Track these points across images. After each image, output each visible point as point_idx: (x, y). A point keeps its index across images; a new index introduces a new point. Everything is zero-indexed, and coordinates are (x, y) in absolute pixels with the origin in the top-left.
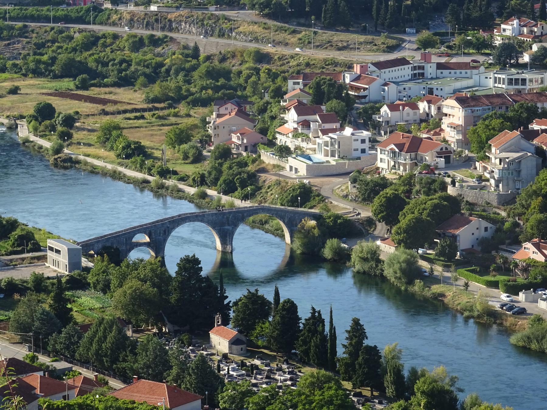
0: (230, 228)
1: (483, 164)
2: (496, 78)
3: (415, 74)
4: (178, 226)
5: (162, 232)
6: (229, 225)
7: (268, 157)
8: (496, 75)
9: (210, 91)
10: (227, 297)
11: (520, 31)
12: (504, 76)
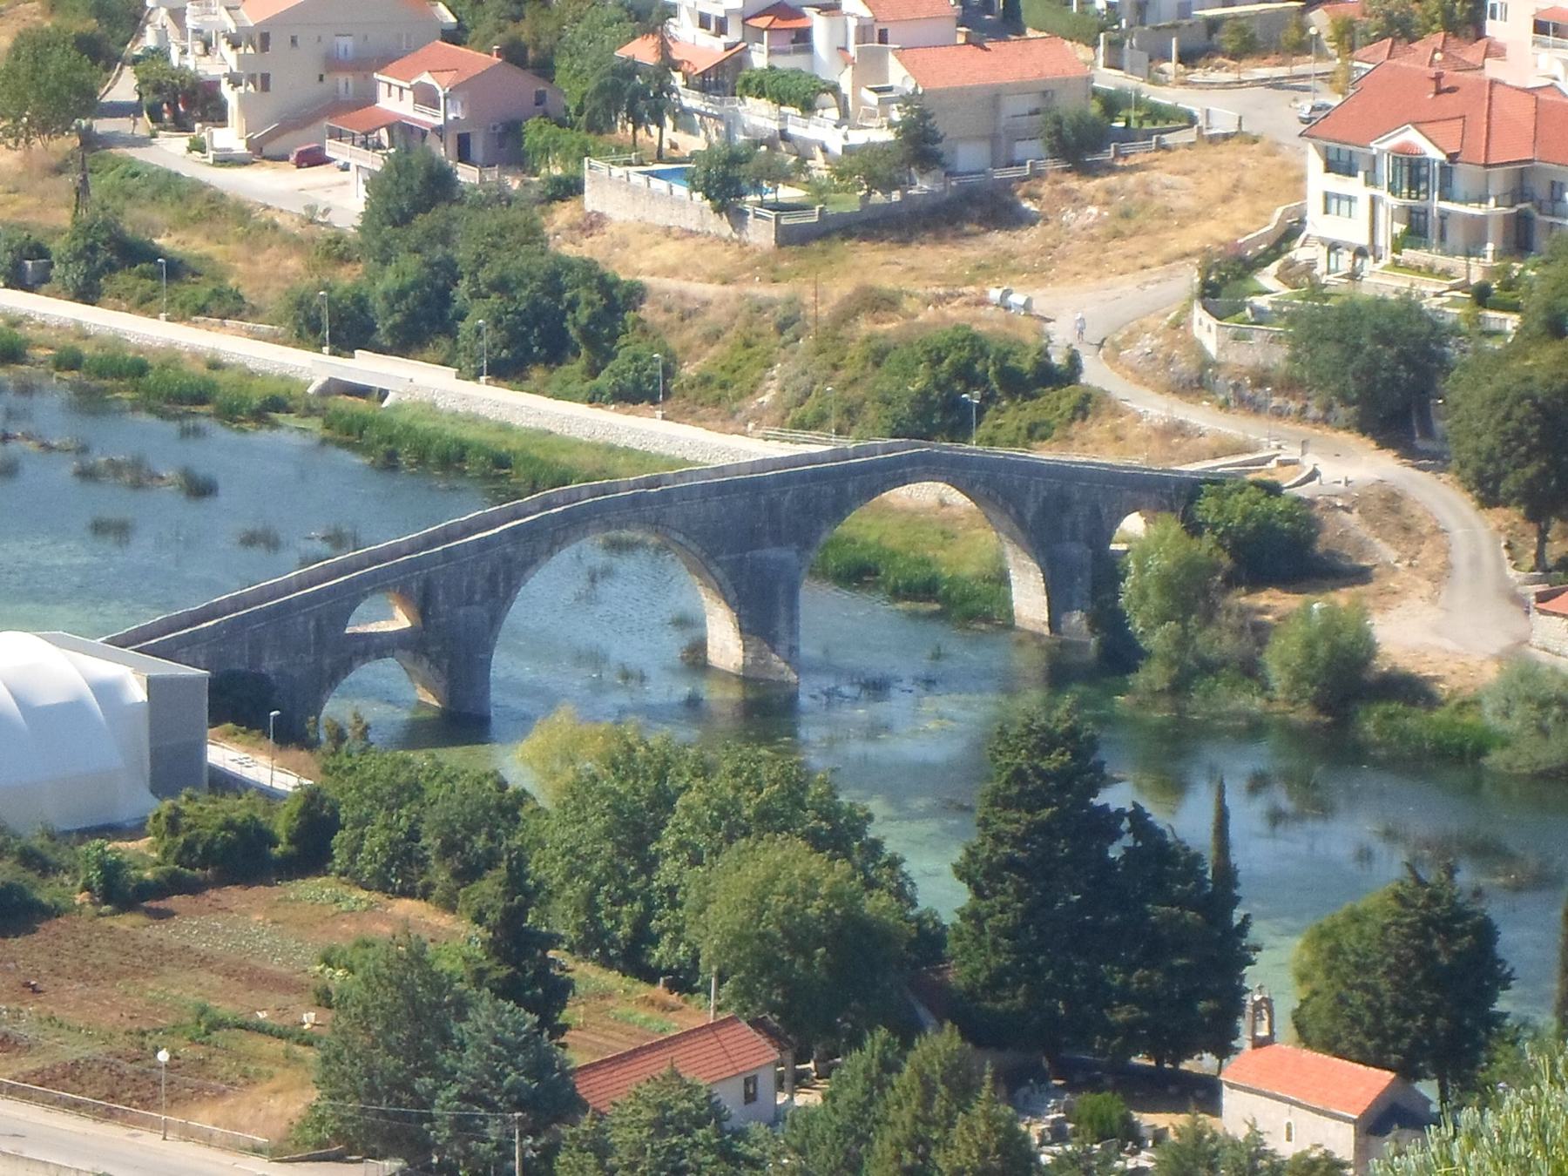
0: (787, 554)
4: (550, 553)
5: (480, 582)
6: (778, 538)
7: (635, 190)
10: (1235, 901)
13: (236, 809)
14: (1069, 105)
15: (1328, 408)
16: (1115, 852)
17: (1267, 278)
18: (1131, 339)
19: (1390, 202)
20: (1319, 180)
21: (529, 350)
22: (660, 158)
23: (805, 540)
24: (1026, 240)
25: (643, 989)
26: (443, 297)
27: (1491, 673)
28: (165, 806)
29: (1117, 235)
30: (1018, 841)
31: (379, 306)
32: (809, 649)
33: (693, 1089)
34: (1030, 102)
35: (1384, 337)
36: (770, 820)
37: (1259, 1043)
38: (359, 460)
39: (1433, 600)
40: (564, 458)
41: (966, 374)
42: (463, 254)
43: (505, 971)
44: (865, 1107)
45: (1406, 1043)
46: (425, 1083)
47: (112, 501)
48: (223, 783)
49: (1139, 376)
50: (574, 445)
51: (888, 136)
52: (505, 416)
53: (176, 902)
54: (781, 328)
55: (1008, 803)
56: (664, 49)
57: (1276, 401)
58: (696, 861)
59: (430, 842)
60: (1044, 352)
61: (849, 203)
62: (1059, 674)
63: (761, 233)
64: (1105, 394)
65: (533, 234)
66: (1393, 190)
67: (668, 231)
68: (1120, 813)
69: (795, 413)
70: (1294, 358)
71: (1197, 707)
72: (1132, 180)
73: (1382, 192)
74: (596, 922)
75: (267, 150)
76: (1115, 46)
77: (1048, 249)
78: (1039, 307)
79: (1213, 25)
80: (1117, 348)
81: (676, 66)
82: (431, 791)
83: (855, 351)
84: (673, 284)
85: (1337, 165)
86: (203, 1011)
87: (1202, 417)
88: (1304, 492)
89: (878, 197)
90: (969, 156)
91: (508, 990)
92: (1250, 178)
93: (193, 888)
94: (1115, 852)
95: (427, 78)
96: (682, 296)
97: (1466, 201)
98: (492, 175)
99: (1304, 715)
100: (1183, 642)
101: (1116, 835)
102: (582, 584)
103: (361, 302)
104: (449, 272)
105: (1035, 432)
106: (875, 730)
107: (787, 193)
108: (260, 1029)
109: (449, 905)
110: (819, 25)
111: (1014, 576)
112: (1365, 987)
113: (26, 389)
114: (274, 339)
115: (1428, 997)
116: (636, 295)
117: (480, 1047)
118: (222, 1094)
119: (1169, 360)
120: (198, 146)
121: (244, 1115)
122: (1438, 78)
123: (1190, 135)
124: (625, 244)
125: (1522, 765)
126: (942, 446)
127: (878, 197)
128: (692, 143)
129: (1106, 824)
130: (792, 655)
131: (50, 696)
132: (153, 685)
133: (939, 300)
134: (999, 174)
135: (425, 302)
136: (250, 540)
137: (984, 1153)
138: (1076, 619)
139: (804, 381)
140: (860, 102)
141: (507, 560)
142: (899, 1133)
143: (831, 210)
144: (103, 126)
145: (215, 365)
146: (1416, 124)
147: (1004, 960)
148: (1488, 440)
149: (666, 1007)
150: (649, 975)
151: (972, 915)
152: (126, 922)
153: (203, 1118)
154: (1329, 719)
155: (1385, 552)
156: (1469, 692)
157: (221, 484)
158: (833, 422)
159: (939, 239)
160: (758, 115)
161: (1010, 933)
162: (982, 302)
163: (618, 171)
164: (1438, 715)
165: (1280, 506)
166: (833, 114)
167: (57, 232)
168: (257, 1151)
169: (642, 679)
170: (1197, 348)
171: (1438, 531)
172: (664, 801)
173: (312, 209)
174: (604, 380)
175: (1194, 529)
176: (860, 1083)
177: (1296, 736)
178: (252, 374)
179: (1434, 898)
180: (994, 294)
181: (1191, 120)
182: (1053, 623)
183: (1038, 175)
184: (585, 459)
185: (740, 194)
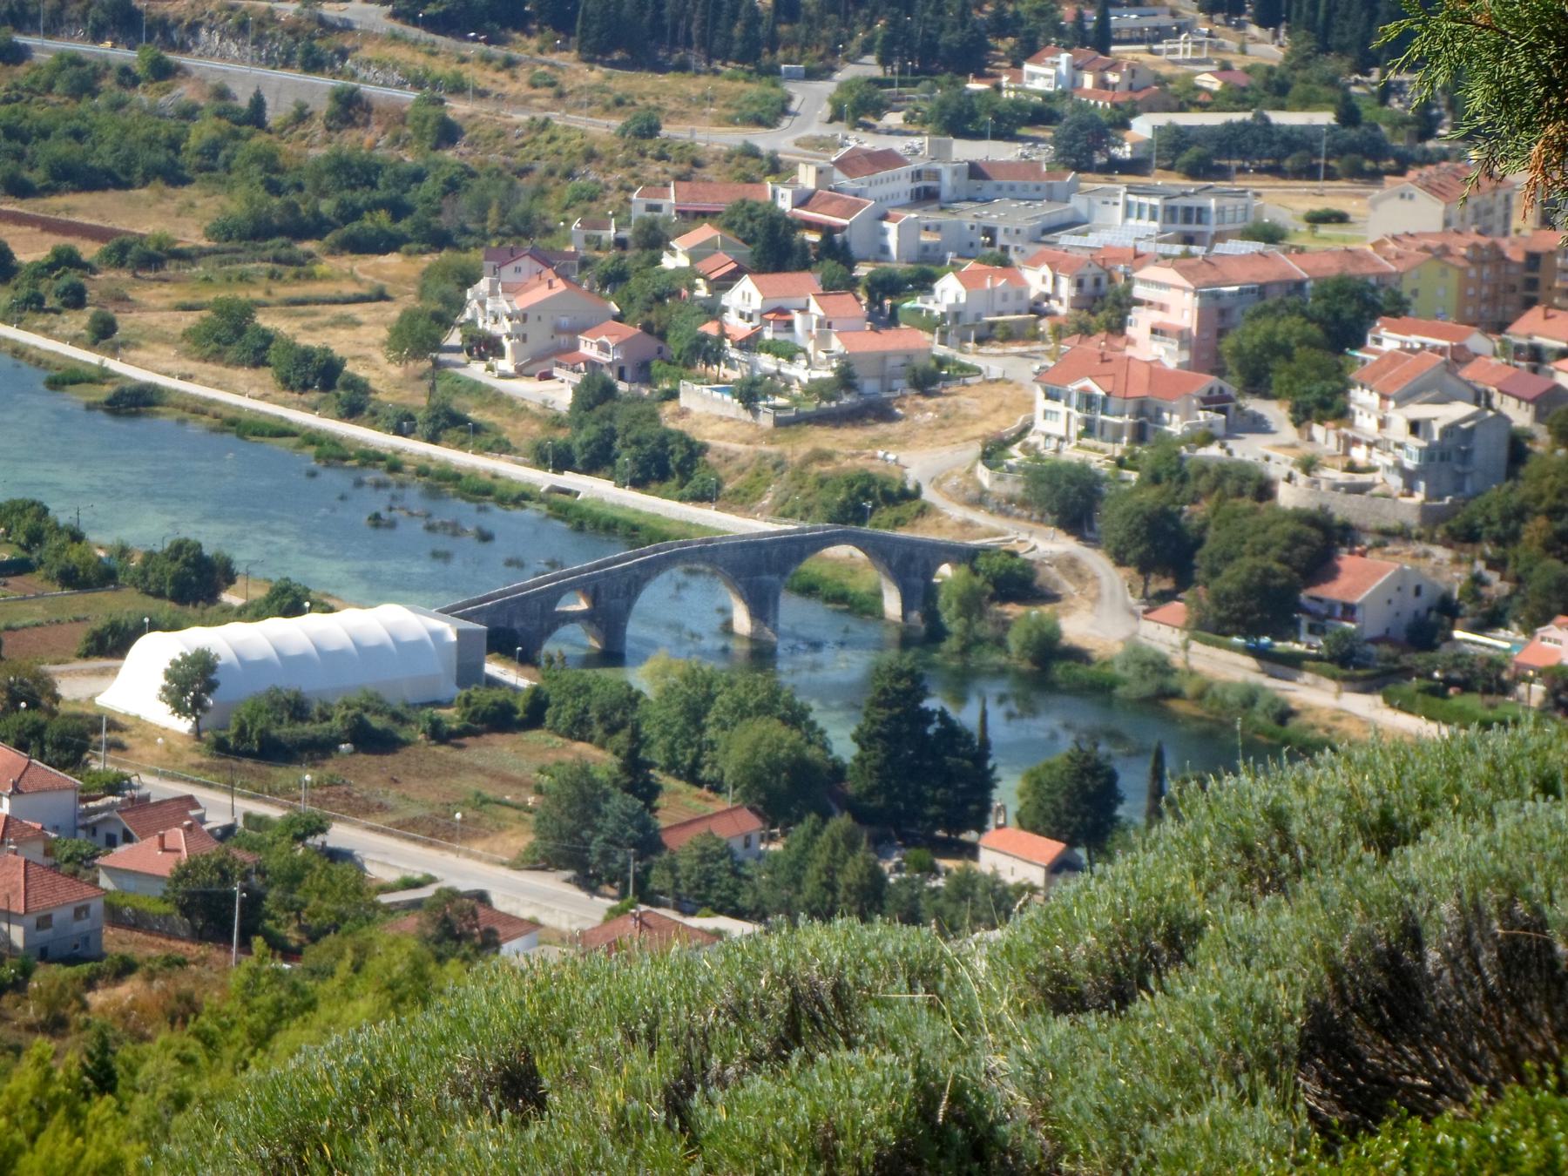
0: (774, 578)
1: (1344, 430)
2: (1128, 205)
3: (918, 190)
4: (657, 574)
6: (770, 572)
7: (704, 397)
8: (1132, 198)
9: (383, 217)
11: (1074, 80)
12: (1155, 201)
13: (498, 695)
14: (920, 362)
15: (1043, 515)
16: (931, 730)
17: (1015, 450)
18: (947, 478)
19: (1077, 415)
20: (1042, 403)
21: (649, 474)
22: (718, 382)
23: (783, 572)
24: (897, 428)
25: (696, 790)
26: (609, 447)
27: (1118, 649)
28: (463, 693)
29: (942, 427)
30: (883, 723)
31: (576, 450)
32: (783, 626)
33: (719, 841)
34: (900, 360)
35: (1071, 481)
36: (764, 709)
37: (999, 827)
38: (564, 526)
39: (1091, 611)
40: (666, 528)
41: (865, 493)
42: (619, 425)
43: (627, 780)
44: (803, 852)
45: (1071, 829)
46: (587, 833)
47: (442, 542)
48: (492, 682)
49: (950, 497)
50: (670, 522)
51: (830, 374)
52: (637, 506)
53: (468, 740)
54: (775, 467)
55: (879, 705)
56: (722, 328)
57: (1017, 511)
58: (724, 728)
59: (593, 714)
60: (903, 483)
61: (810, 407)
62: (906, 641)
63: (766, 420)
64: (932, 505)
65: (654, 417)
66: (1078, 409)
67: (720, 418)
68: (934, 712)
69: (781, 509)
70: (1026, 490)
71: (973, 662)
72: (950, 400)
73: (1073, 410)
74: (674, 756)
75: (526, 371)
76: (944, 334)
77: (906, 433)
78: (902, 461)
79: (992, 325)
80: (940, 483)
81: (727, 336)
82: (596, 689)
83: (811, 480)
84: (722, 444)
85: (1051, 396)
86: (478, 794)
87: (980, 518)
88: (1030, 556)
89: (824, 404)
90: (870, 386)
91: (630, 789)
92: (1008, 401)
93: (476, 734)
94: (931, 730)
95: (604, 339)
96: (726, 450)
97: (1114, 415)
98: (635, 387)
99: (1026, 666)
100: (968, 628)
101: (931, 722)
102: (671, 590)
103: (568, 448)
104: (612, 434)
105: (898, 522)
106: (815, 667)
107: (780, 401)
108: (507, 805)
109: (602, 746)
110: (797, 318)
111: (886, 593)
112: (1052, 801)
113: (402, 485)
114: (525, 464)
115: (1084, 807)
116: (704, 448)
117: (616, 817)
118: (486, 836)
119: (965, 489)
120: (490, 368)
121: (497, 846)
122: (1102, 355)
123: (979, 379)
124: (699, 423)
125: (1133, 694)
126: (852, 528)
127: (824, 404)
128: (735, 375)
129: (927, 717)
130: (775, 629)
131: (408, 636)
132: (460, 633)
133: (853, 456)
134: (886, 395)
135: (600, 448)
136: (509, 563)
137: (861, 876)
138: (915, 616)
139: (785, 494)
140: (817, 357)
141: (637, 577)
142: (820, 865)
143: (802, 410)
144: (444, 357)
145: (495, 477)
146: (1091, 377)
147: (874, 782)
148: (1121, 533)
149: (707, 800)
150: (699, 783)
151: (860, 760)
152: (442, 750)
153: (477, 847)
154: (1036, 668)
155: (1068, 587)
156: (1107, 658)
157: (497, 536)
158: (799, 514)
159: (854, 425)
160: (767, 362)
161: (877, 769)
162: (874, 458)
163: (697, 387)
164: (1093, 668)
165: (1017, 562)
166: (804, 363)
167: (419, 409)
168: (503, 864)
169: (701, 638)
170: (978, 484)
171: (1095, 578)
172: (710, 698)
173: (545, 401)
174: (687, 490)
175: (976, 572)
176: (801, 841)
177: (1021, 677)
178: (513, 482)
179: (1087, 758)
180: (880, 453)
181: (979, 372)
182: (904, 616)
183: (904, 396)
184: (675, 528)
185: (756, 400)
